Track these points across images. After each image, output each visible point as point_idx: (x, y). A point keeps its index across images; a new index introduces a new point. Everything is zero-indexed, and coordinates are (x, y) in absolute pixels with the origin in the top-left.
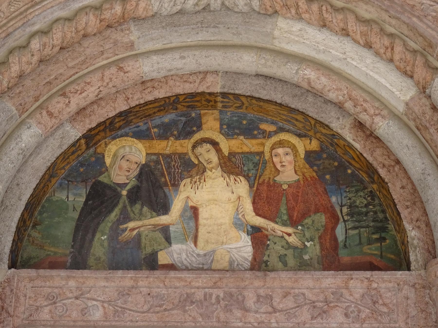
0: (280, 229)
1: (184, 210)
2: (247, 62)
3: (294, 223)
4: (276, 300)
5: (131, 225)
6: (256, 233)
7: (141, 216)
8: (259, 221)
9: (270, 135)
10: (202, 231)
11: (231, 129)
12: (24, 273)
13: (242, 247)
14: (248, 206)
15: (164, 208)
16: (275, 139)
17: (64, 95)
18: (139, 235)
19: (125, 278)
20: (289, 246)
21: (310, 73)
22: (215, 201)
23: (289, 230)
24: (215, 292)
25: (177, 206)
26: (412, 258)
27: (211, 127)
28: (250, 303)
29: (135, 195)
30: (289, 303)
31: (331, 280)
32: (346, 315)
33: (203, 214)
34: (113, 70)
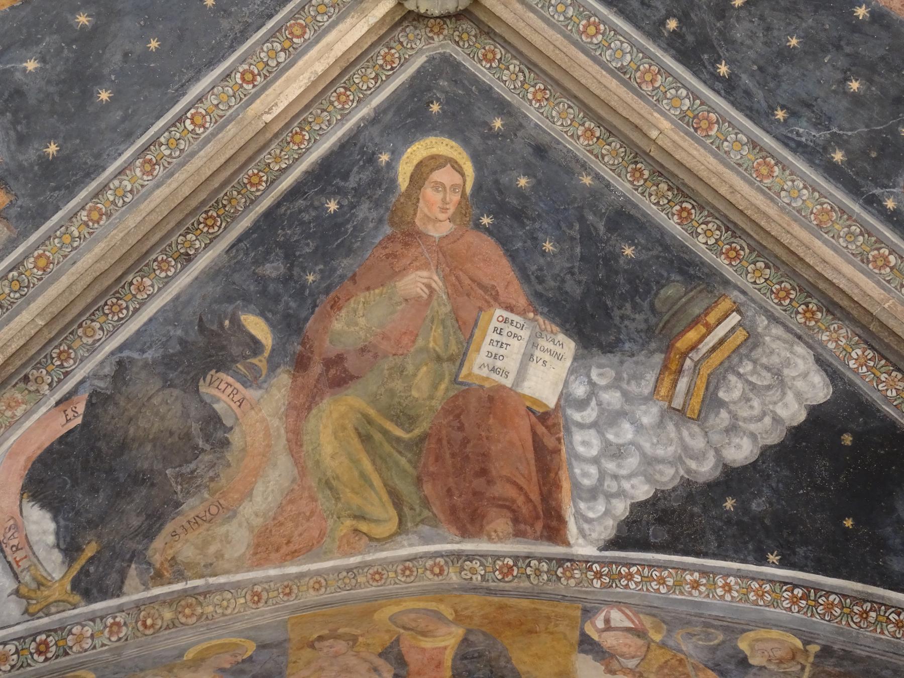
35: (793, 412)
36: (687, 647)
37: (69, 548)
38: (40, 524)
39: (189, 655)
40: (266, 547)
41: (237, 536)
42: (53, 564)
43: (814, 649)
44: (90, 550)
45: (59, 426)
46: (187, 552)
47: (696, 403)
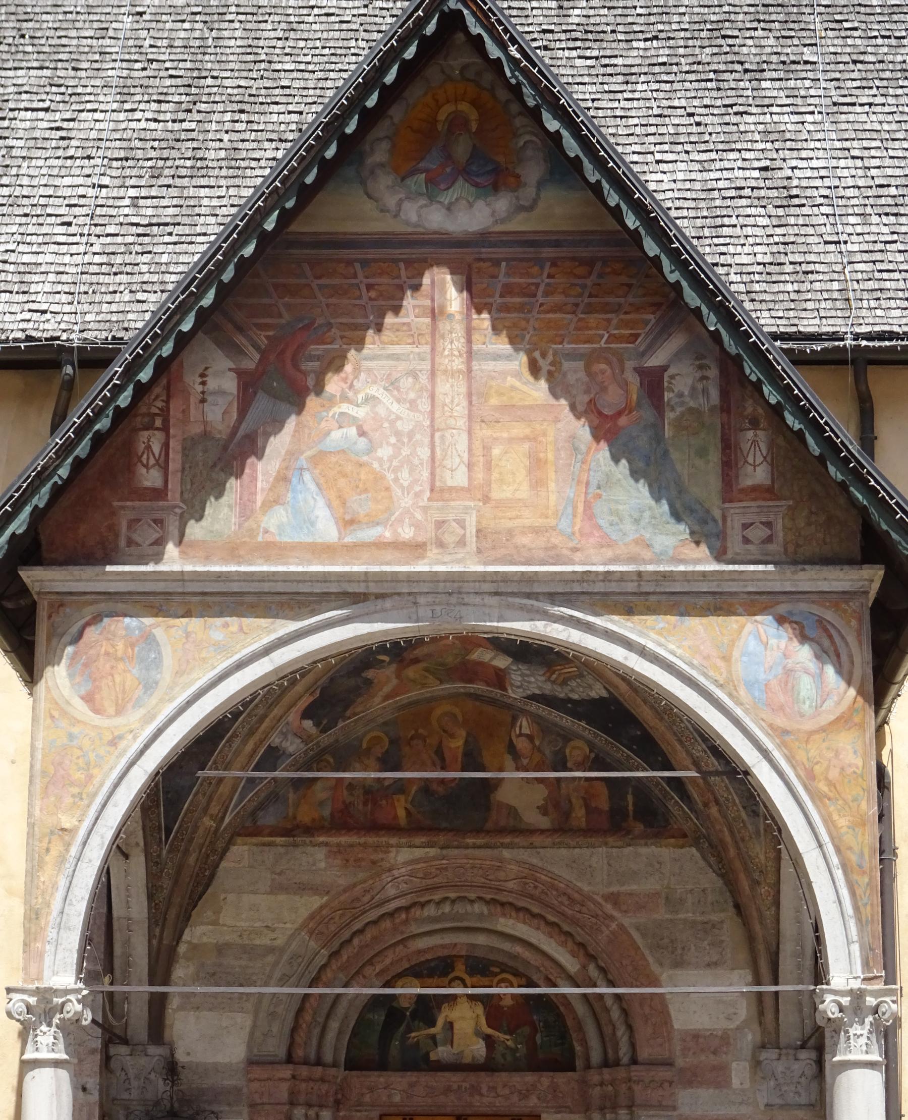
0: (502, 1036)
1: (445, 1024)
2: (481, 939)
3: (510, 1032)
4: (499, 1090)
5: (413, 1034)
6: (489, 1040)
7: (419, 1029)
8: (490, 1031)
9: (496, 974)
10: (455, 1037)
11: (471, 973)
12: (354, 1073)
13: (479, 1049)
14: (483, 1021)
15: (433, 1024)
16: (500, 977)
17: (372, 964)
18: (418, 1041)
19: (411, 1076)
20: (507, 1047)
21: (518, 949)
22: (463, 1018)
23: (508, 1037)
24: (464, 1085)
25: (440, 1022)
26: (577, 1063)
27: (460, 970)
28: (484, 1090)
29: (415, 1015)
30: (507, 1091)
31: (530, 1078)
32: (539, 1098)
33: (456, 1026)
34: (401, 947)
35: (594, 694)
36: (547, 752)
37: (317, 725)
38: (308, 724)
39: (364, 746)
40: (387, 697)
41: (377, 699)
42: (314, 731)
43: (593, 755)
44: (325, 722)
45: (312, 699)
46: (358, 710)
47: (559, 681)
